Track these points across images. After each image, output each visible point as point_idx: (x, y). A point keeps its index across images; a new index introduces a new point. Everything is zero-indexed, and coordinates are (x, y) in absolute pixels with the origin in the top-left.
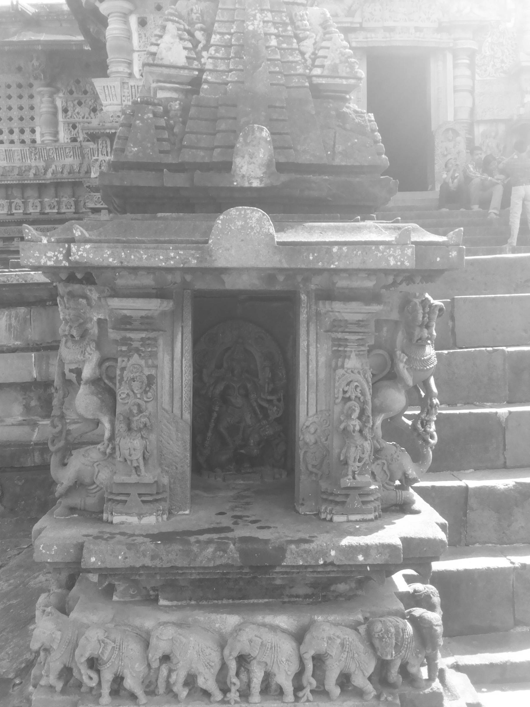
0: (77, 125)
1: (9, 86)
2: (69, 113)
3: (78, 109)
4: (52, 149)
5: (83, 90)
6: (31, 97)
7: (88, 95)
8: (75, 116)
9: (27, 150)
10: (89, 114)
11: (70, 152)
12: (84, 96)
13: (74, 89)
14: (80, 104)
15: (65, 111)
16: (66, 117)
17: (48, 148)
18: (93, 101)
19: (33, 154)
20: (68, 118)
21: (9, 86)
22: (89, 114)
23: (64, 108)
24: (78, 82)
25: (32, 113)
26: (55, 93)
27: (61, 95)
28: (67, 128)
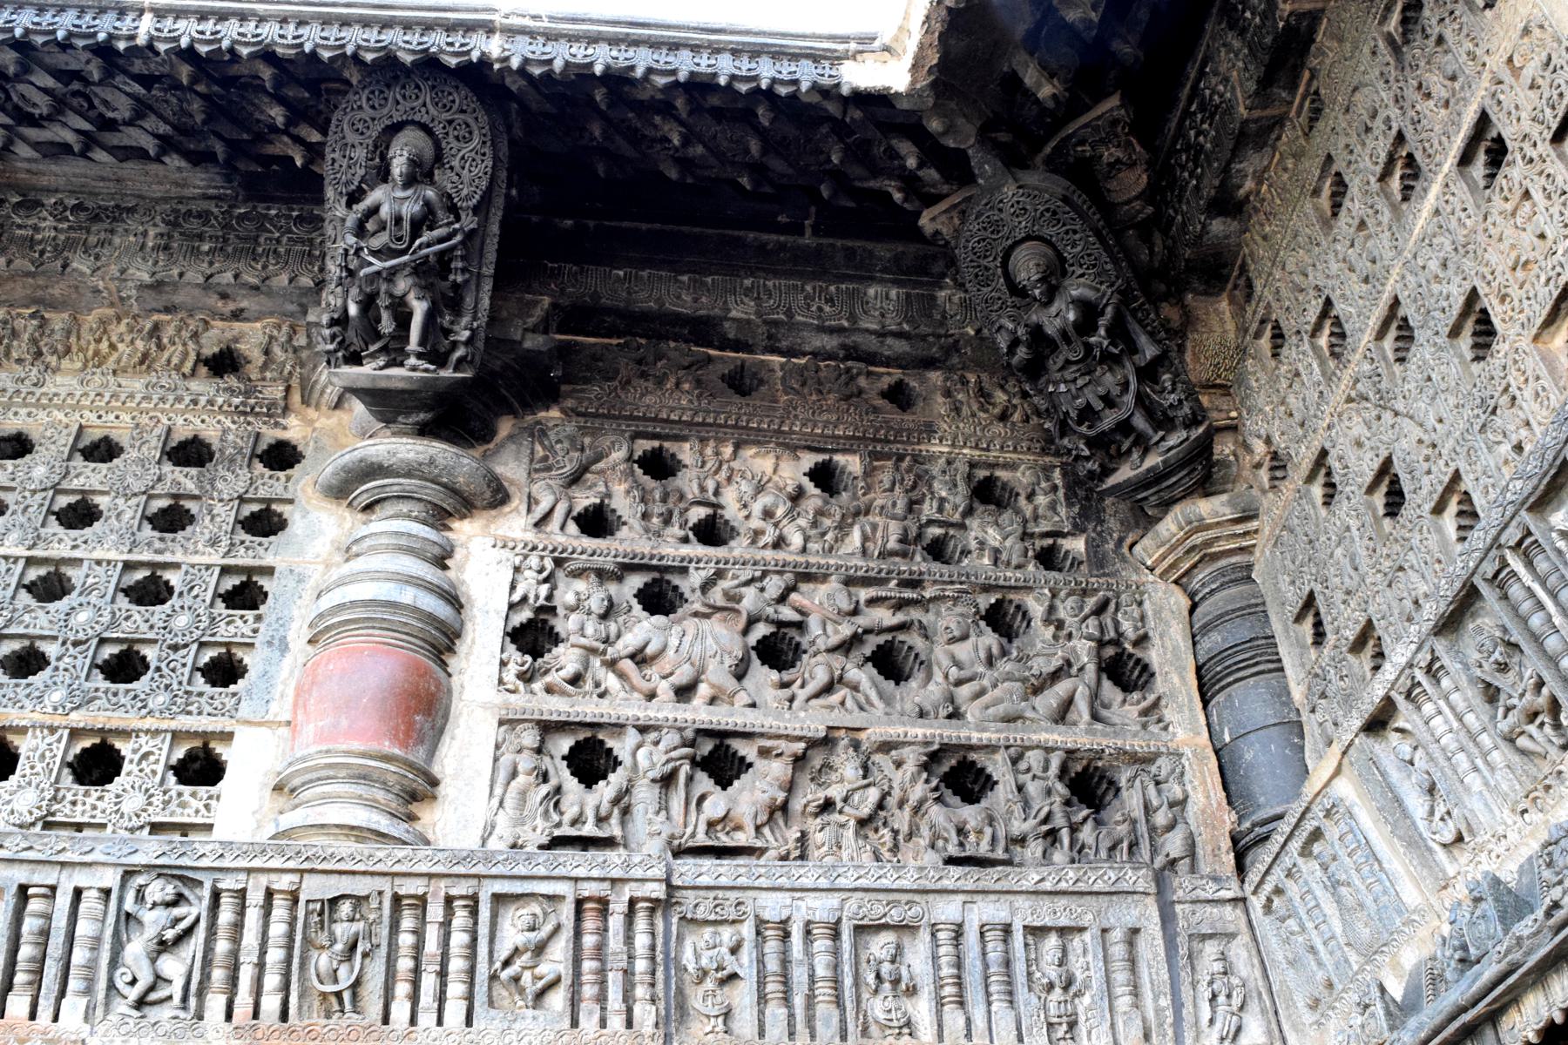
0: (622, 747)
1: (103, 451)
2: (565, 659)
3: (642, 629)
4: (359, 901)
5: (698, 514)
6: (265, 523)
7: (738, 548)
8: (611, 681)
9: (90, 901)
10: (740, 674)
11: (540, 949)
12: (697, 550)
13: (623, 503)
14: (659, 599)
15: (533, 636)
16: (527, 677)
17: (316, 888)
18: (774, 585)
19: (136, 949)
20: (549, 690)
21: (103, 451)
22: (740, 674)
23: (525, 615)
24: (659, 466)
25: (235, 626)
26: (466, 505)
27: (515, 524)
28: (526, 762)
